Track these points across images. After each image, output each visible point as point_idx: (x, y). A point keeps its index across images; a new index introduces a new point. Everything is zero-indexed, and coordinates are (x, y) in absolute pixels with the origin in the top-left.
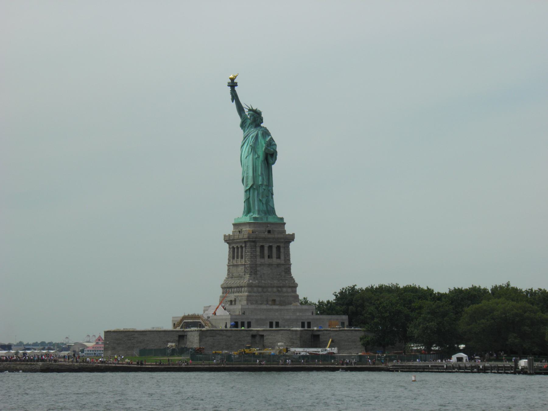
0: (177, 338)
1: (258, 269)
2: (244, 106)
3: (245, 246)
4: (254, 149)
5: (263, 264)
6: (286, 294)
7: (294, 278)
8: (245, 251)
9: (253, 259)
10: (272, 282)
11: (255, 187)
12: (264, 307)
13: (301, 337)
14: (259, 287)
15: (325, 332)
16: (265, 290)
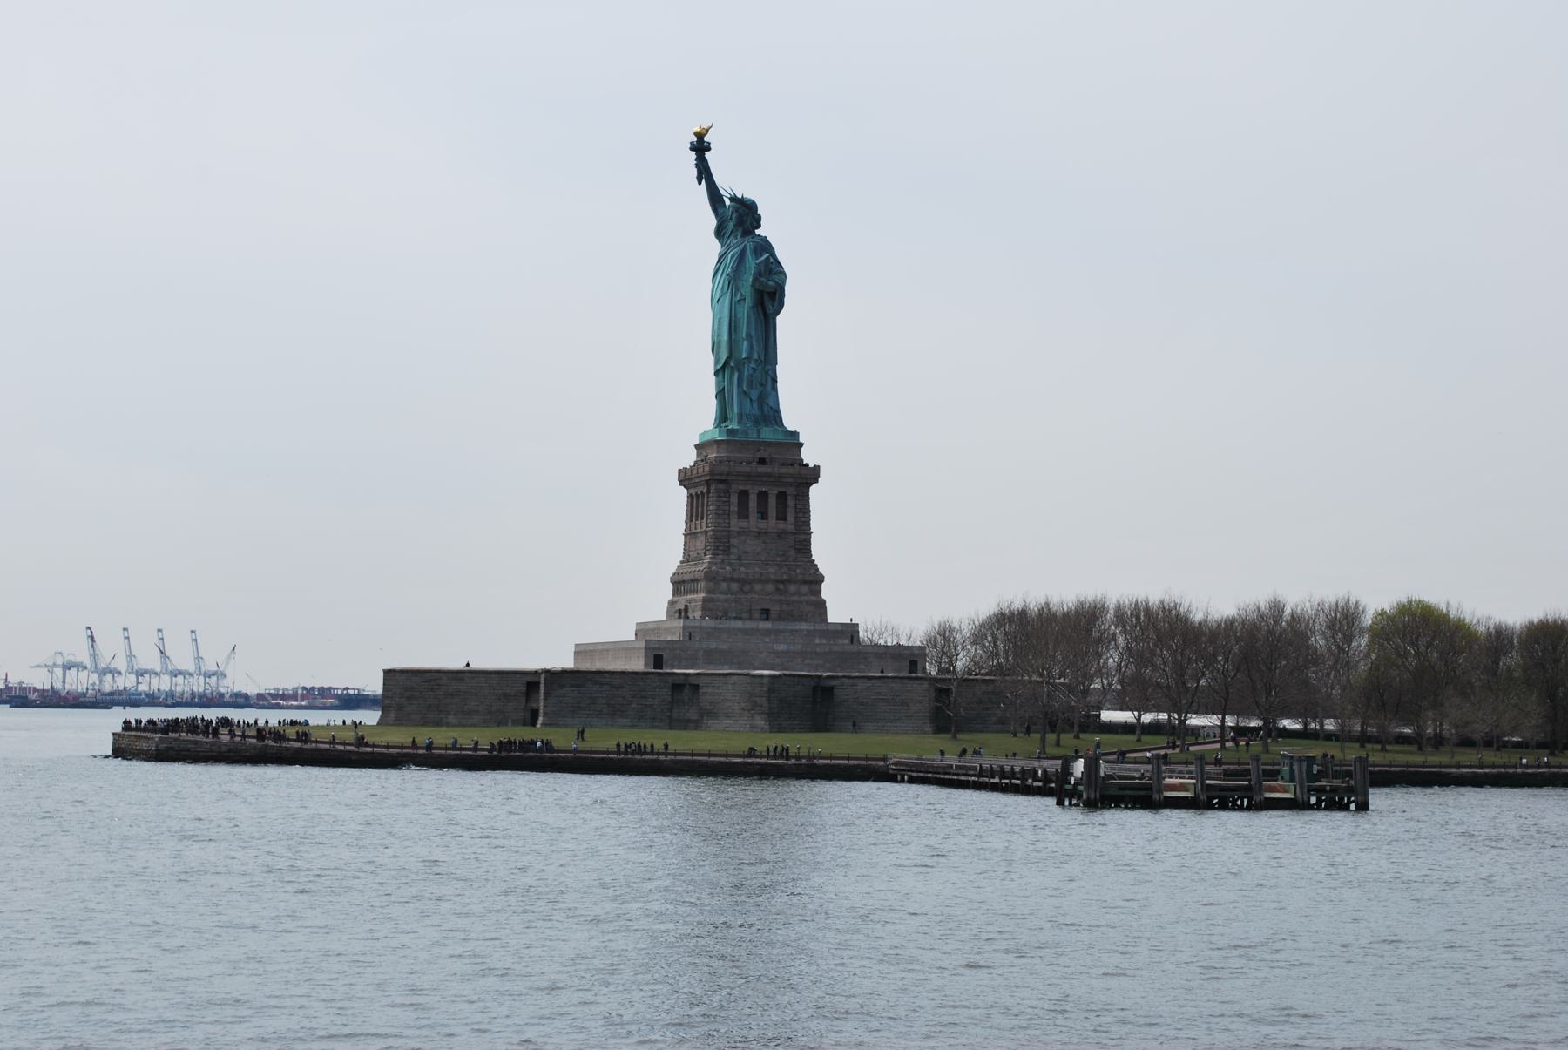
0: (524, 689)
1: (734, 541)
2: (723, 192)
3: (708, 492)
4: (734, 281)
5: (744, 532)
6: (795, 598)
7: (816, 563)
8: (708, 502)
9: (721, 521)
10: (763, 571)
11: (732, 365)
12: (739, 624)
13: (771, 691)
14: (732, 579)
15: (846, 681)
16: (747, 588)
